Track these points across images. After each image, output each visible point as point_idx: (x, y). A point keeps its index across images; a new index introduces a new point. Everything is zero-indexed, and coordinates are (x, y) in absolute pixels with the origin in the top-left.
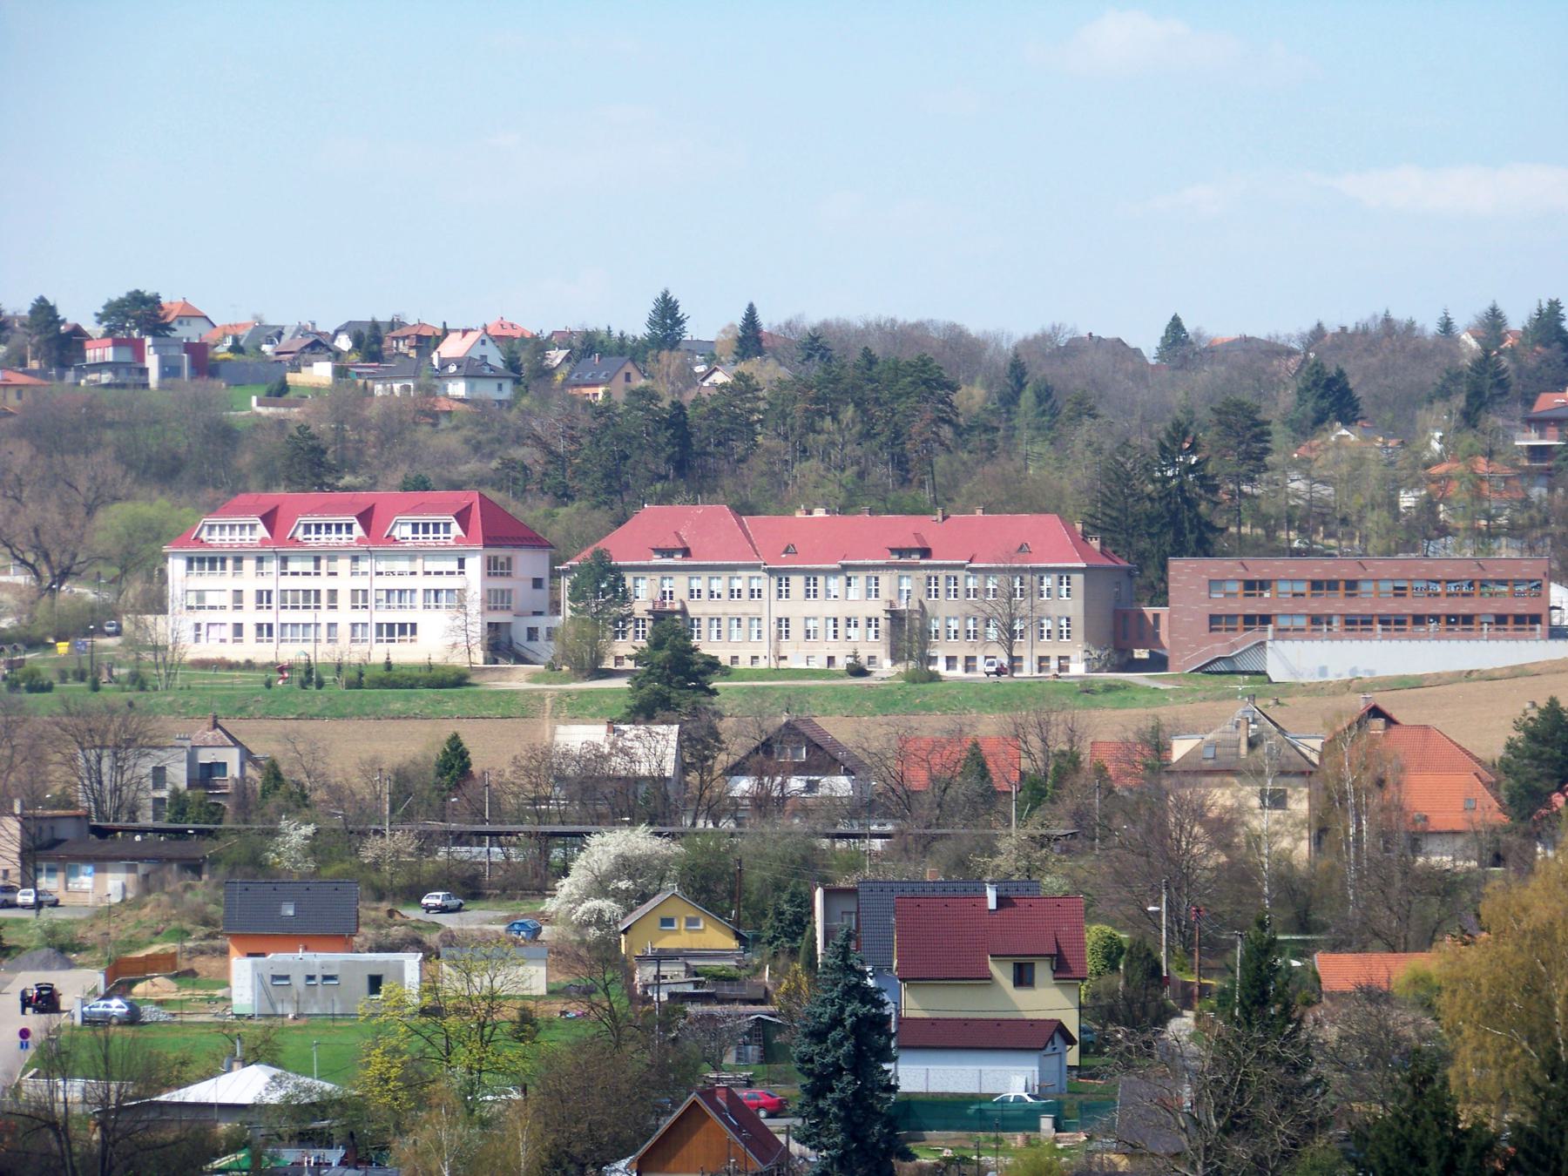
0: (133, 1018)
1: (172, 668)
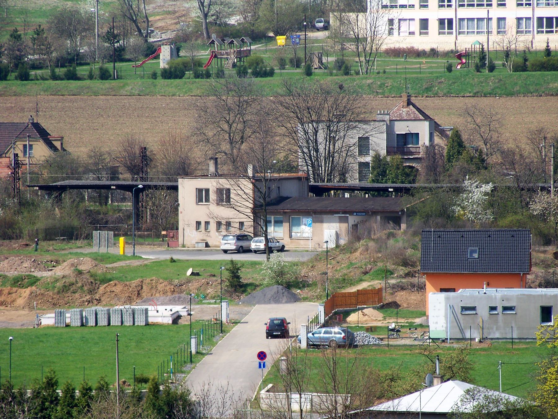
0: (349, 342)
1: (371, 55)
